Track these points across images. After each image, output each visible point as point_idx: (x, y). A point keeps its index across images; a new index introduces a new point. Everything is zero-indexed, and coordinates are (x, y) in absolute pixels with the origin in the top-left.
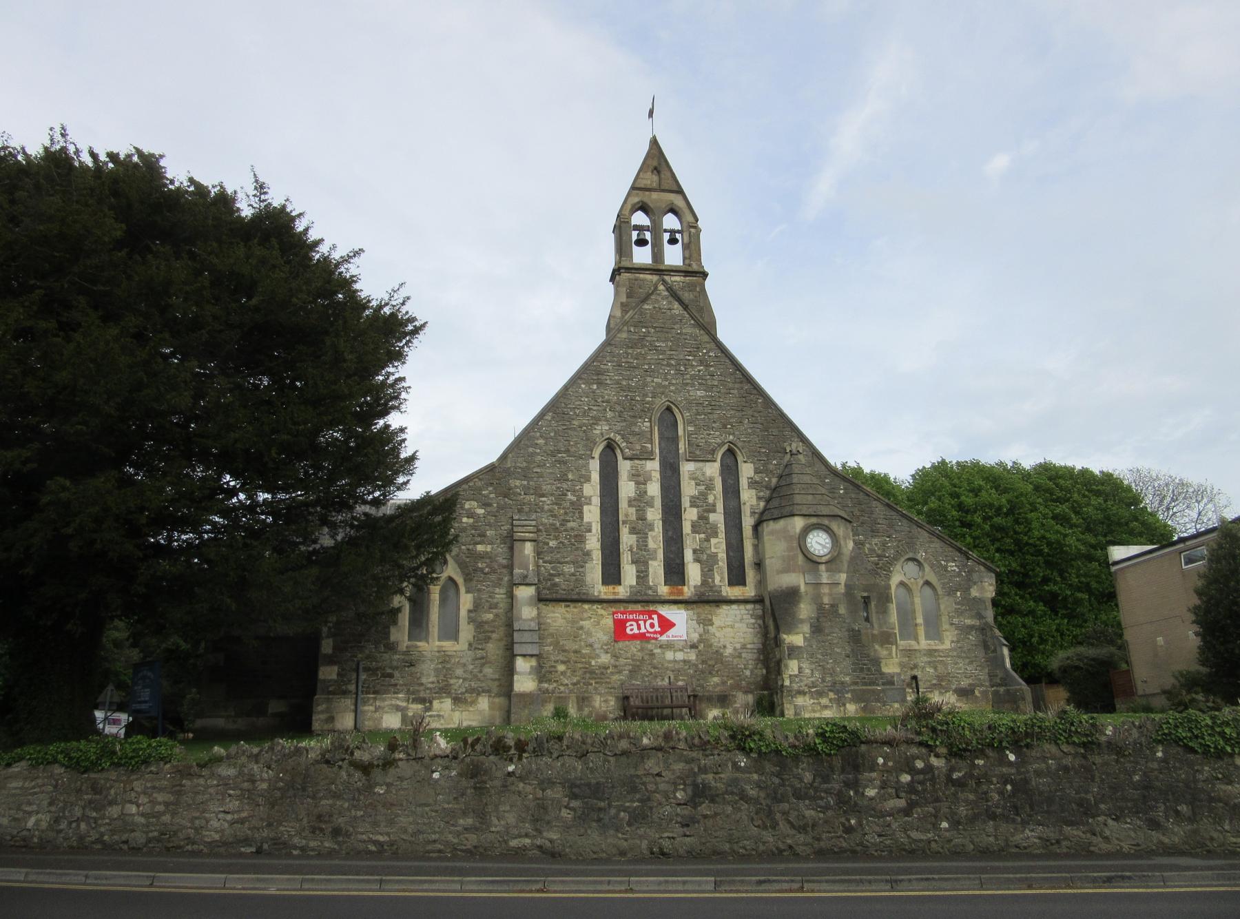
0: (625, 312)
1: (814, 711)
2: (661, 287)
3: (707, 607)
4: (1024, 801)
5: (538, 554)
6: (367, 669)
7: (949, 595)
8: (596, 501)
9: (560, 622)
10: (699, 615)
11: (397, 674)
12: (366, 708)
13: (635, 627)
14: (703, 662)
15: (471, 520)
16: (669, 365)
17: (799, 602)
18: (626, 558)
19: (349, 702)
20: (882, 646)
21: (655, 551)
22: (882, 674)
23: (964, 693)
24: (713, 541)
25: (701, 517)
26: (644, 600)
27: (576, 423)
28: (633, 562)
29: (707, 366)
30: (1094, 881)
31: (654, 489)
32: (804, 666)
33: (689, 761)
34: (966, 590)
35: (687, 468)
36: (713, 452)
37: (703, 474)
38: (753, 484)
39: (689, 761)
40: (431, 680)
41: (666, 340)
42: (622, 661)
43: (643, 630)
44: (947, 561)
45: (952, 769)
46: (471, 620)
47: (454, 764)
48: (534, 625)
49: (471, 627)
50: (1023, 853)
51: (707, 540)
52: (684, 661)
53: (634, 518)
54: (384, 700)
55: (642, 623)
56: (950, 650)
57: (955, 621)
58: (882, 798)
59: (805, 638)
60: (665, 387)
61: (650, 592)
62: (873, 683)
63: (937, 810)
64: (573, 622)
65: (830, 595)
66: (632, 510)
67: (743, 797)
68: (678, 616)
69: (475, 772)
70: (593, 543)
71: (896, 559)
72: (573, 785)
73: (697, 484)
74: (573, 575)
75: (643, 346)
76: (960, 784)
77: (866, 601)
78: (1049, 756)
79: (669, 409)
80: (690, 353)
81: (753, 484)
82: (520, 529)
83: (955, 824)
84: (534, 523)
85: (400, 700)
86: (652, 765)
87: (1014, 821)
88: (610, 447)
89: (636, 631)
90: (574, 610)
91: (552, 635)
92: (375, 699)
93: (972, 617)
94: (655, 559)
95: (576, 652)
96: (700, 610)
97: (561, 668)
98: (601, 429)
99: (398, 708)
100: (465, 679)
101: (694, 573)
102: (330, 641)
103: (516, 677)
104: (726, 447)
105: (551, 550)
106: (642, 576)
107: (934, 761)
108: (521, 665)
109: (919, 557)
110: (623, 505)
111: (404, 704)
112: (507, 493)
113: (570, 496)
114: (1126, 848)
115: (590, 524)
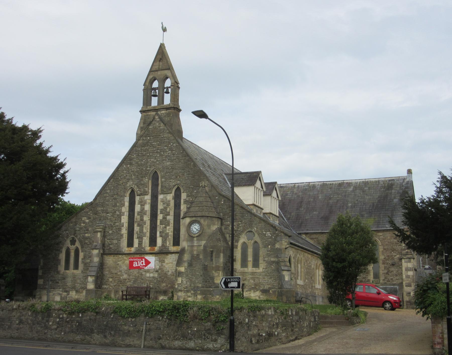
0: (141, 131)
2: (157, 117)
3: (163, 255)
5: (104, 236)
6: (51, 280)
7: (265, 247)
8: (126, 214)
9: (111, 262)
11: (60, 282)
13: (136, 264)
14: (160, 277)
15: (84, 225)
16: (157, 152)
17: (184, 253)
18: (135, 236)
19: (46, 292)
20: (216, 271)
21: (146, 233)
22: (214, 283)
23: (265, 292)
24: (168, 228)
25: (164, 218)
26: (140, 253)
27: (121, 182)
28: (138, 238)
29: (172, 150)
31: (147, 207)
32: (183, 280)
34: (274, 245)
35: (161, 197)
36: (171, 189)
37: (166, 199)
38: (186, 202)
39: (21, 313)
42: (131, 277)
43: (139, 265)
46: (83, 262)
48: (97, 264)
49: (83, 265)
51: (165, 227)
52: (153, 277)
53: (139, 220)
54: (56, 291)
55: (139, 262)
56: (263, 272)
57: (266, 259)
58: (52, 325)
60: (155, 162)
61: (143, 250)
62: (210, 287)
65: (197, 250)
66: (139, 217)
68: (152, 259)
70: (124, 231)
71: (242, 232)
73: (164, 204)
74: (117, 244)
76: (68, 322)
77: (212, 252)
78: (90, 315)
79: (156, 172)
80: (166, 146)
81: (186, 202)
83: (65, 333)
84: (102, 224)
85: (60, 291)
86: (14, 314)
87: (76, 333)
88: (133, 192)
89: (137, 265)
90: (116, 257)
91: (108, 267)
93: (274, 257)
94: (145, 236)
95: (116, 274)
96: (160, 257)
97: (111, 280)
98: (130, 184)
99: (59, 294)
100: (80, 284)
101: (159, 241)
103: (88, 284)
104: (176, 187)
105: (110, 235)
106: (140, 244)
107: (65, 316)
108: (90, 279)
110: (136, 214)
111: (61, 293)
113: (117, 213)
114: (97, 343)
115: (123, 223)
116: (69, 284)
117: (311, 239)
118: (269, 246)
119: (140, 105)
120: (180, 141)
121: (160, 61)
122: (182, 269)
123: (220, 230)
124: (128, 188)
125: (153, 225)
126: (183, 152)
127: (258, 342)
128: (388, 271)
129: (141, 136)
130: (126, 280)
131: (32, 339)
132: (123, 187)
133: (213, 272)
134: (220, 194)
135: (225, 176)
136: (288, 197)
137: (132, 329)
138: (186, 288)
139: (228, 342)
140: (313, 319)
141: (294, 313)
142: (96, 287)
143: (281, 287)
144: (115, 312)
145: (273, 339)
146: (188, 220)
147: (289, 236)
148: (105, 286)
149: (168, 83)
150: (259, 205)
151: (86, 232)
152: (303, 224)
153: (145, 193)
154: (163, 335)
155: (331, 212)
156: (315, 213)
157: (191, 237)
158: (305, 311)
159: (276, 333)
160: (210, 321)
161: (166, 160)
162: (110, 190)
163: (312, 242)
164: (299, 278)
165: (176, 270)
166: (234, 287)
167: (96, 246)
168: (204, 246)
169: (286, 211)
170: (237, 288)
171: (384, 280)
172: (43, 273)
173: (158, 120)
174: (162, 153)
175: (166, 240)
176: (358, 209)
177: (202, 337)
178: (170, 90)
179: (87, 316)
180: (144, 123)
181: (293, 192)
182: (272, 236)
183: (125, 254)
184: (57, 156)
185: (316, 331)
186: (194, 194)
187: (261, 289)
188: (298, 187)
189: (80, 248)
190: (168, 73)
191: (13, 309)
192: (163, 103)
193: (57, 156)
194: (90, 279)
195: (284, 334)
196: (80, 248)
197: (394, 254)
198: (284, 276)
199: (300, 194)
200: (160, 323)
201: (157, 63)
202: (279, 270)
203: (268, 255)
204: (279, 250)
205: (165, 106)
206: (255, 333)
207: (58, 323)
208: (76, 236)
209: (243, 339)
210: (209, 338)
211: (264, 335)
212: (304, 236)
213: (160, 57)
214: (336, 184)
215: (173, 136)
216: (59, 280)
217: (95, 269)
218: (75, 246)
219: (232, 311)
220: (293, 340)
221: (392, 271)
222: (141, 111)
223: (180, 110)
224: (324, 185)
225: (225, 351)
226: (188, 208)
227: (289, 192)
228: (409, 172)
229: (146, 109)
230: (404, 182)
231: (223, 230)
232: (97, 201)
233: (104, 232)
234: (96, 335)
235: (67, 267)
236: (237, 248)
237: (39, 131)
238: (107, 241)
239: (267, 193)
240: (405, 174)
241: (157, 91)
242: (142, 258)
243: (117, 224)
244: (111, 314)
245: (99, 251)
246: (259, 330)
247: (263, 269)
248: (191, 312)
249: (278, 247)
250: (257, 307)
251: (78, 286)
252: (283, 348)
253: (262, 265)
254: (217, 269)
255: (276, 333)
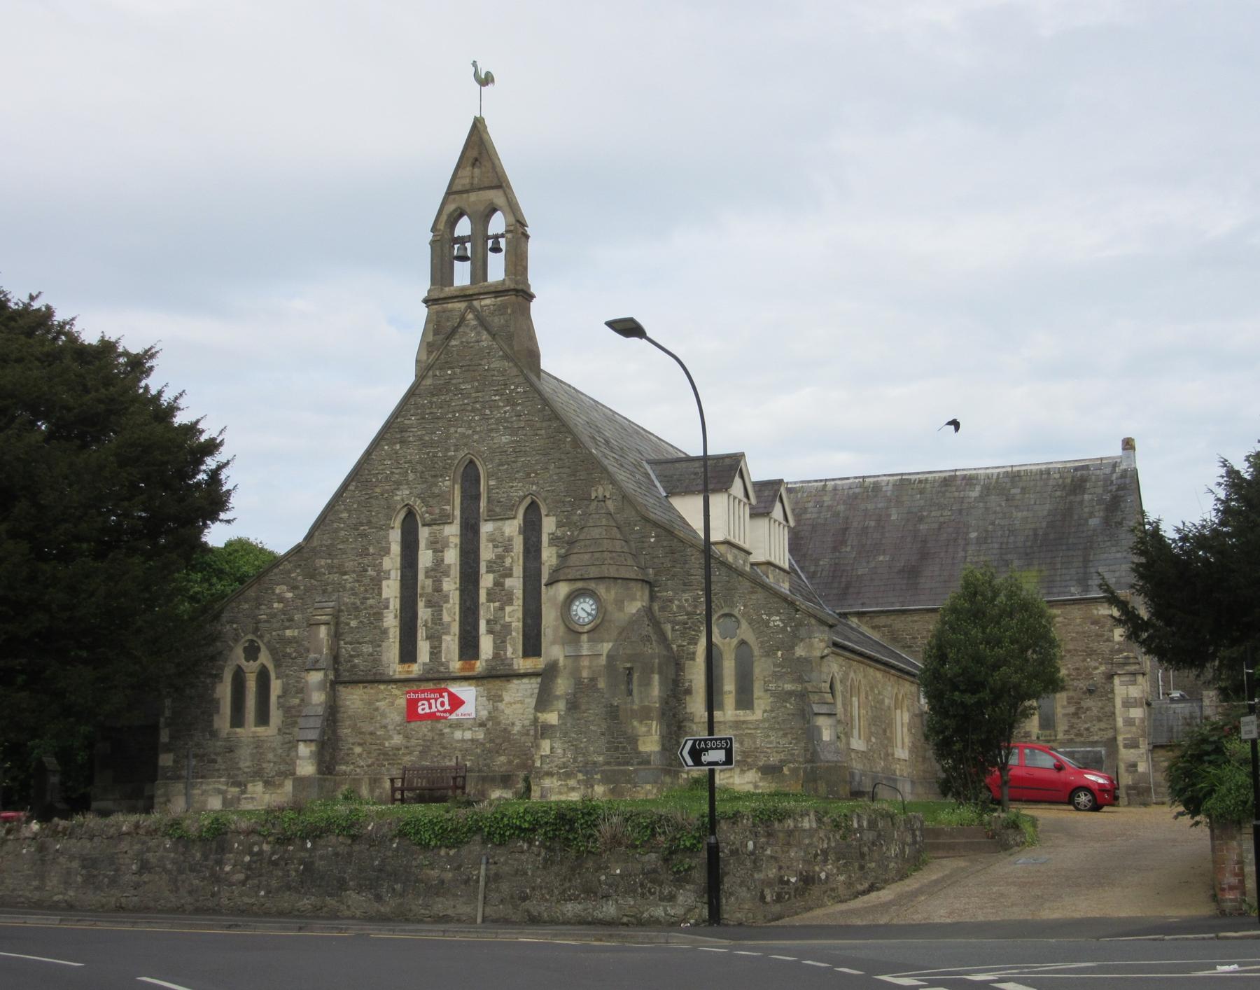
0: (430, 353)
1: (560, 793)
2: (470, 316)
3: (498, 683)
4: (310, 877)
5: (336, 636)
6: (196, 756)
7: (768, 655)
8: (395, 575)
9: (358, 704)
10: (489, 690)
11: (219, 759)
12: (196, 792)
13: (427, 706)
14: (492, 741)
15: (281, 605)
18: (421, 633)
20: (641, 722)
21: (449, 624)
23: (770, 771)
24: (508, 609)
25: (498, 584)
26: (437, 678)
27: (378, 490)
28: (427, 638)
29: (514, 405)
30: (222, 927)
31: (452, 557)
32: (555, 745)
33: (144, 843)
35: (486, 528)
36: (514, 507)
38: (554, 540)
39: (144, 843)
40: (248, 764)
41: (473, 379)
42: (413, 742)
43: (434, 709)
44: (770, 615)
45: (273, 853)
46: (280, 706)
47: (33, 843)
48: (320, 711)
49: (280, 712)
50: (301, 915)
51: (502, 609)
52: (472, 740)
53: (429, 590)
54: (208, 784)
56: (763, 721)
57: (772, 686)
58: (233, 872)
59: (560, 716)
60: (468, 436)
61: (442, 669)
62: (627, 763)
63: (260, 882)
64: (370, 703)
65: (590, 667)
66: (429, 582)
67: (164, 869)
69: (42, 849)
70: (391, 621)
72: (85, 859)
73: (495, 547)
74: (371, 655)
75: (448, 391)
76: (275, 863)
77: (630, 671)
78: (334, 843)
79: (471, 462)
81: (554, 540)
82: (320, 612)
83: (268, 892)
84: (332, 604)
86: (124, 846)
89: (427, 711)
90: (371, 691)
91: (350, 717)
92: (201, 783)
93: (793, 681)
94: (448, 633)
95: (371, 734)
96: (490, 686)
97: (358, 750)
98: (402, 494)
99: (219, 792)
101: (486, 645)
102: (167, 731)
104: (527, 501)
105: (352, 630)
106: (435, 653)
107: (266, 847)
108: (304, 750)
109: (736, 612)
110: (421, 576)
111: (224, 788)
112: (312, 574)
113: (371, 572)
114: (358, 913)
115: (387, 600)
116: (245, 764)
117: (873, 628)
118: (779, 653)
119: (423, 286)
120: (534, 379)
121: (473, 165)
122: (552, 718)
123: (649, 611)
124: (399, 507)
125: (468, 604)
126: (543, 409)
127: (779, 898)
128: (1078, 709)
129: (430, 367)
130: (399, 749)
131: (179, 910)
132: (383, 502)
133: (635, 723)
134: (646, 520)
135: (648, 467)
136: (808, 516)
137: (450, 875)
138: (565, 766)
139: (705, 899)
140: (909, 840)
141: (865, 824)
142: (320, 771)
143: (813, 757)
144: (402, 834)
145: (816, 890)
146: (563, 589)
147: (831, 626)
148: (344, 768)
149: (497, 224)
150: (741, 543)
151: (287, 624)
152: (851, 590)
153: (445, 519)
154: (533, 889)
155: (924, 555)
156: (881, 558)
157: (572, 633)
158: (892, 817)
159: (823, 876)
160: (654, 849)
161: (497, 430)
162: (349, 511)
163: (875, 636)
164: (856, 732)
165: (536, 720)
166: (716, 763)
167: (317, 661)
168: (608, 656)
169: (804, 555)
170: (724, 764)
171: (1066, 732)
172: (172, 737)
173: (474, 323)
174: (488, 412)
175: (504, 642)
176: (996, 546)
177: (635, 891)
178: (502, 242)
179: (326, 846)
180: (436, 332)
181: (820, 504)
182: (785, 626)
183: (395, 681)
184: (198, 421)
185: (917, 868)
186: (575, 518)
187: (761, 764)
188: (835, 489)
189: (271, 667)
190: (496, 197)
191: (121, 835)
192: (485, 279)
193: (198, 421)
194: (304, 750)
195: (842, 878)
196: (271, 667)
197: (1094, 664)
198: (818, 730)
199: (841, 508)
200: (524, 857)
201: (467, 171)
202: (805, 715)
203: (777, 677)
204: (805, 661)
205: (491, 285)
206: (771, 876)
207: (248, 867)
208: (261, 637)
209: (743, 893)
210: (652, 894)
211: (793, 880)
212: (854, 621)
213: (474, 153)
214: (935, 481)
215: (516, 365)
216: (217, 754)
217: (318, 722)
218: (258, 662)
219: (712, 822)
220: (864, 893)
221: (1088, 709)
222: (426, 301)
223: (531, 297)
224: (904, 484)
225: (697, 924)
226: (563, 558)
227: (811, 504)
228: (1128, 444)
229: (442, 296)
230: (1113, 471)
231: (657, 613)
232: (315, 543)
233: (337, 624)
234: (354, 895)
235: (238, 719)
236: (693, 659)
237: (149, 354)
238: (346, 649)
239: (761, 511)
240: (1116, 451)
241: (468, 245)
242: (440, 692)
243: (370, 602)
244: (391, 840)
245: (326, 675)
246: (780, 868)
247: (765, 711)
248: (605, 828)
249: (803, 654)
250: (775, 812)
251: (269, 769)
252: (842, 912)
253: (761, 701)
254: (645, 714)
255: (823, 876)
